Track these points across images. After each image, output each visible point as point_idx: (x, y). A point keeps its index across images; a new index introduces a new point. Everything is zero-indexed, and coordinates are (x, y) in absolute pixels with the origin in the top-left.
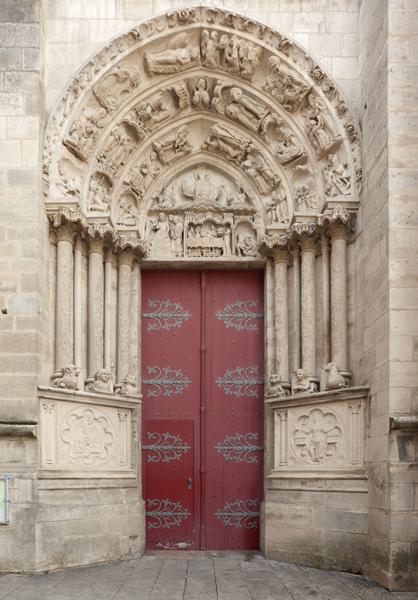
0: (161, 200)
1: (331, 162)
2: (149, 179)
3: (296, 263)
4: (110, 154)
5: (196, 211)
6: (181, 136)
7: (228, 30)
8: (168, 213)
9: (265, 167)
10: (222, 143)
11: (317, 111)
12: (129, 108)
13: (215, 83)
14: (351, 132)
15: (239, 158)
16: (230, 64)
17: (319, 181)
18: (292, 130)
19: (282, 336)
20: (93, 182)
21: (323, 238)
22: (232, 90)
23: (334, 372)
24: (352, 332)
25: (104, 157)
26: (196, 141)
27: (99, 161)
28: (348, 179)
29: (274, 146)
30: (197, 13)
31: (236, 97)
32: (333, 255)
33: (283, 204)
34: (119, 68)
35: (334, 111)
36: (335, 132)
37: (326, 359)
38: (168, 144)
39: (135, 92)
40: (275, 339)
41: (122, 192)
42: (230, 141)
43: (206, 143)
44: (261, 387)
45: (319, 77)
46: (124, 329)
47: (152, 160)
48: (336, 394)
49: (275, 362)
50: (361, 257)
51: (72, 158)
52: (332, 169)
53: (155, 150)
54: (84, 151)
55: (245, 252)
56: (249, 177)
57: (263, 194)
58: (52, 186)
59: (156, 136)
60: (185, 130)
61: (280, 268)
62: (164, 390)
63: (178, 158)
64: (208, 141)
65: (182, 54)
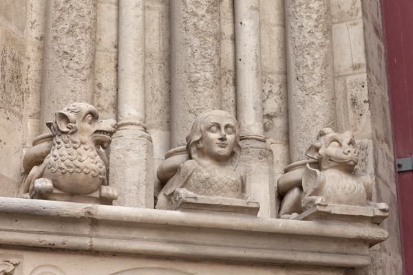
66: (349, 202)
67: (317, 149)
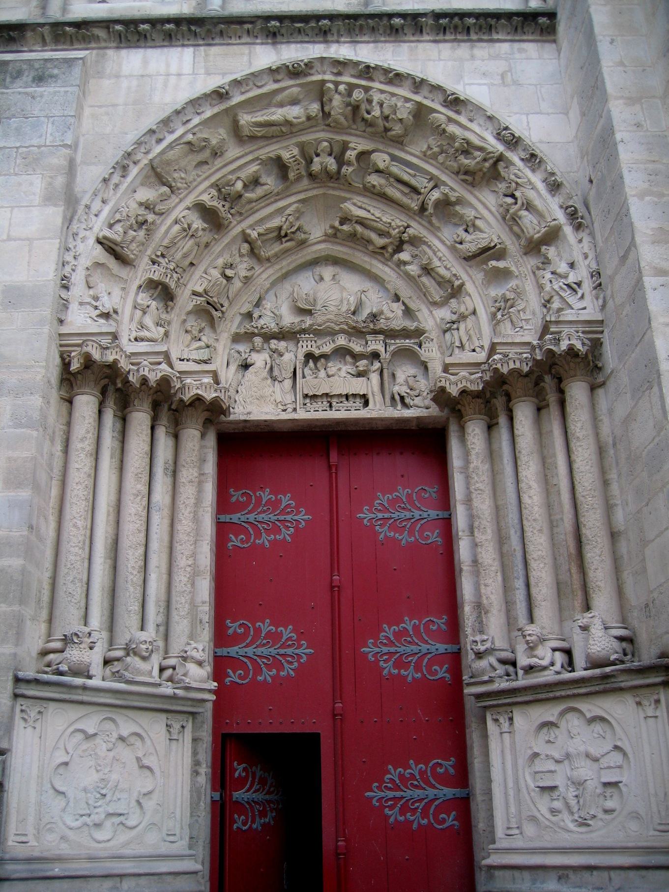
0: (255, 315)
1: (547, 258)
2: (237, 284)
3: (503, 420)
4: (173, 250)
5: (317, 333)
6: (291, 218)
7: (363, 83)
8: (268, 337)
9: (436, 263)
10: (359, 228)
11: (514, 185)
12: (207, 184)
13: (345, 147)
14: (573, 215)
15: (390, 250)
16: (369, 124)
17: (529, 287)
18: (476, 209)
19: (489, 556)
20: (141, 295)
21: (547, 378)
22: (374, 156)
23: (597, 630)
24: (623, 547)
25: (163, 256)
26: (316, 229)
27: (154, 263)
28: (579, 284)
29: (449, 233)
30: (317, 65)
31: (381, 165)
32: (569, 409)
33: (470, 321)
34: (194, 134)
35: (541, 186)
36: (547, 215)
37: (578, 602)
38: (269, 231)
39: (219, 163)
40: (475, 562)
41: (190, 307)
42: (375, 224)
43: (332, 227)
44: (456, 660)
45: (513, 142)
46: (183, 549)
47: (241, 256)
48: (605, 677)
49: (480, 607)
50: (621, 411)
51: (111, 262)
52: (551, 268)
53: (246, 239)
54: (130, 252)
55: (407, 400)
56: (408, 276)
57: (435, 304)
58: (74, 306)
59: (251, 220)
60: (297, 211)
61: (475, 431)
62: (258, 670)
63: (286, 251)
64: (337, 224)
65: (294, 112)
66: (200, 682)
67: (186, 652)
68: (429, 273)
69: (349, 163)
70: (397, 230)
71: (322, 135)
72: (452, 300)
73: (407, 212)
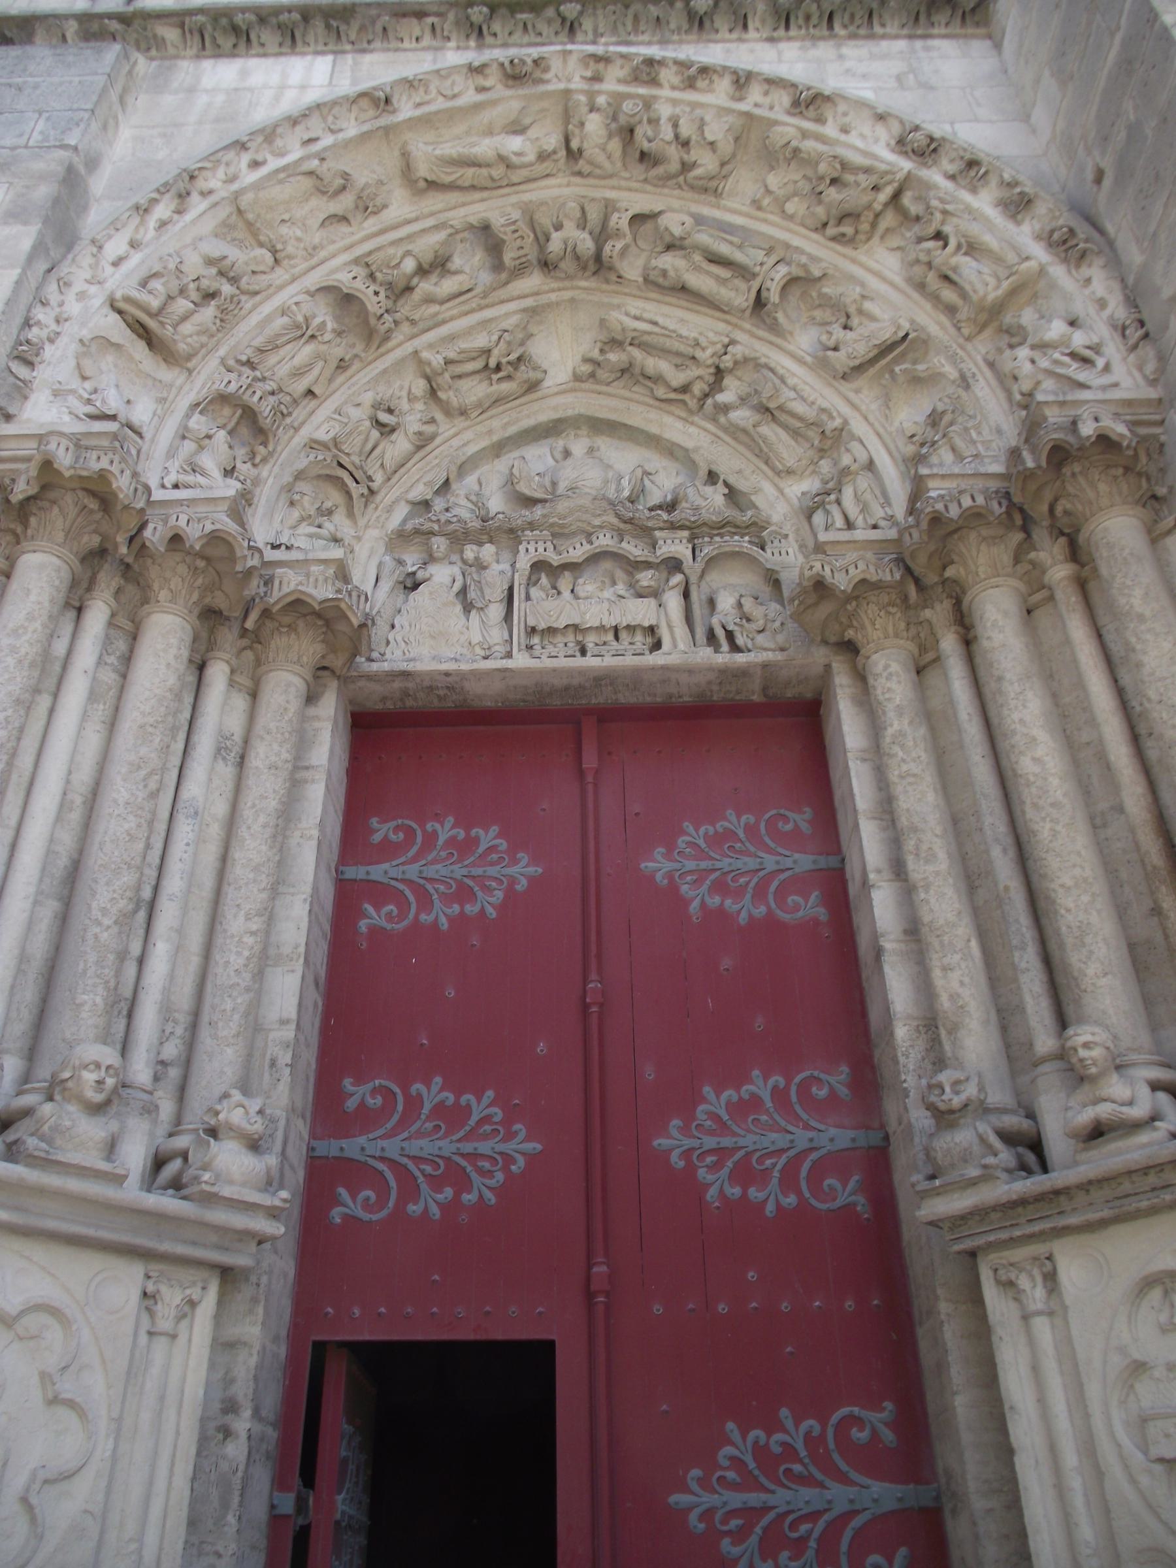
10: (636, 353)
18: (862, 284)
43: (587, 360)
57: (790, 472)
68: (774, 418)
69: (618, 234)
70: (709, 352)
71: (566, 191)
72: (822, 462)
73: (728, 317)
